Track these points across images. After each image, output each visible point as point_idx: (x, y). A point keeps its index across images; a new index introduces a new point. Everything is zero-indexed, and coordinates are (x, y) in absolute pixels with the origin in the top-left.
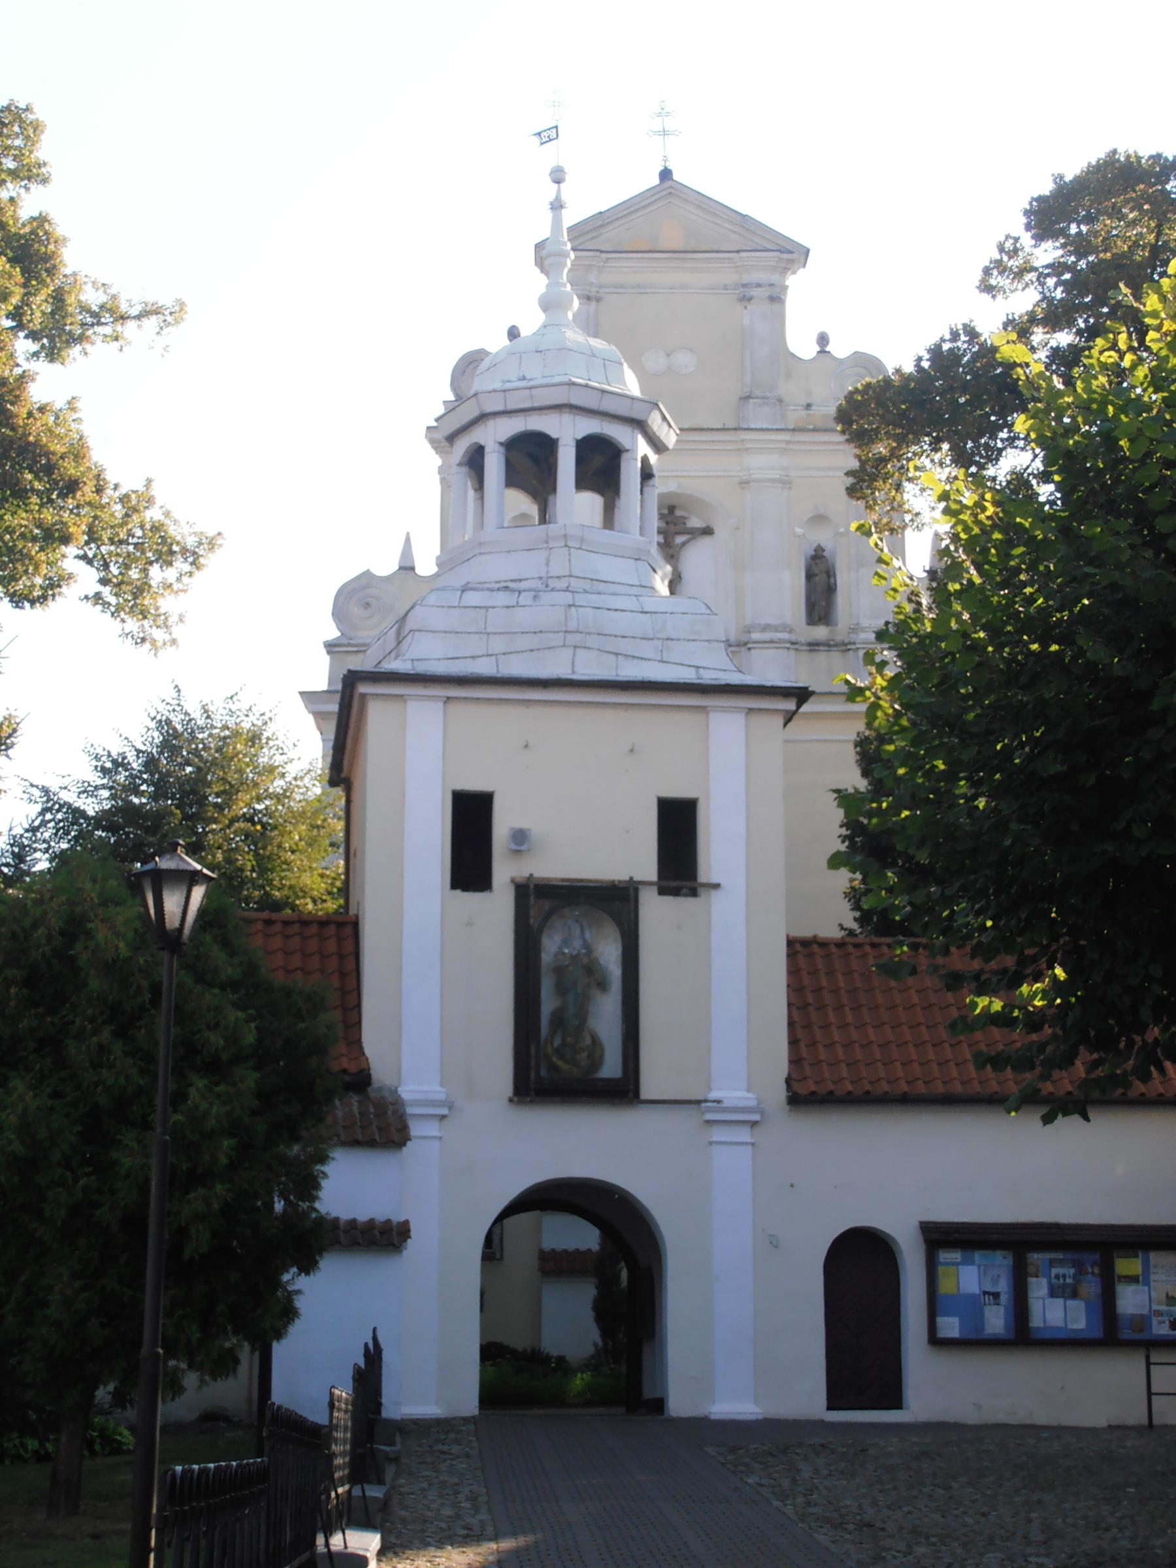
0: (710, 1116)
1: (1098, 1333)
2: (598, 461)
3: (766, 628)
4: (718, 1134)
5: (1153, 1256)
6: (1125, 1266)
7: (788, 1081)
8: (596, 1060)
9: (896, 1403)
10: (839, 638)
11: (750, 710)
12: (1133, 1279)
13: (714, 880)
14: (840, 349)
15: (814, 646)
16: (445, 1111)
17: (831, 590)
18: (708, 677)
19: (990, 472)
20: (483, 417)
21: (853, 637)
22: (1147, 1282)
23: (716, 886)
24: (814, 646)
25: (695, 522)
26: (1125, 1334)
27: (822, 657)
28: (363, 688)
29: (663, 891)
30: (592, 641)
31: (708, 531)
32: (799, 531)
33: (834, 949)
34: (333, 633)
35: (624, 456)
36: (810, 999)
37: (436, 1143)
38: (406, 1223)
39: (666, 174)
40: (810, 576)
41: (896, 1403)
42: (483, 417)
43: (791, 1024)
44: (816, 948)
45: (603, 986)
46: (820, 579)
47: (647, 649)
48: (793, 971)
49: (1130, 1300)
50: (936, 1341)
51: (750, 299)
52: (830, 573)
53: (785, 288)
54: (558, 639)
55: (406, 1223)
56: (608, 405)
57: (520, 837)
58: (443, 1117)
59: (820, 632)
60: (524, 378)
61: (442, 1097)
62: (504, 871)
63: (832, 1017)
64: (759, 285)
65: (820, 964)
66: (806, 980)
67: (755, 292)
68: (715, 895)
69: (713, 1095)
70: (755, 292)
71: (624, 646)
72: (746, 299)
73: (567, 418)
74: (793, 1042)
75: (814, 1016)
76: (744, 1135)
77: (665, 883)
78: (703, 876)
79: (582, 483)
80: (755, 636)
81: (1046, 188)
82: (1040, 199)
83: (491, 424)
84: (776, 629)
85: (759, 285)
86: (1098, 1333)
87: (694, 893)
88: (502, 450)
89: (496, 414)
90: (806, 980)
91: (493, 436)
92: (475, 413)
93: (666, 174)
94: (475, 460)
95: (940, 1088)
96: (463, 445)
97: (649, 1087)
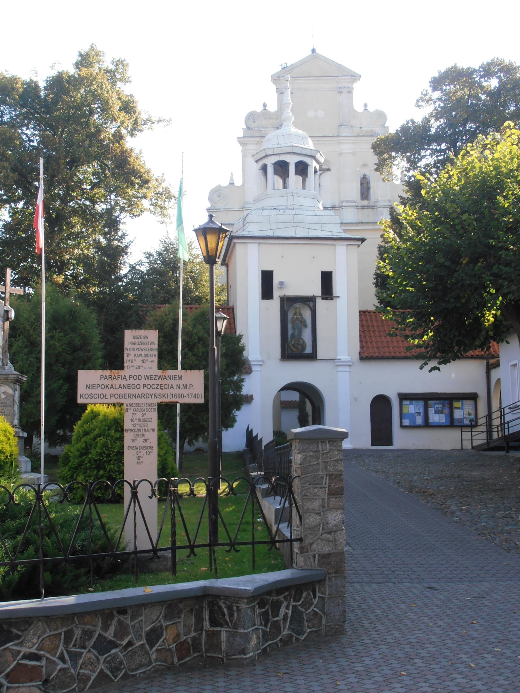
0: (337, 364)
1: (448, 424)
2: (301, 167)
3: (348, 202)
4: (340, 369)
5: (464, 401)
6: (456, 404)
7: (360, 353)
8: (304, 347)
9: (391, 444)
10: (371, 204)
11: (348, 245)
12: (459, 408)
13: (338, 295)
14: (371, 109)
15: (363, 207)
16: (261, 363)
17: (369, 188)
18: (335, 235)
19: (418, 165)
20: (266, 156)
21: (376, 204)
22: (463, 409)
23: (339, 297)
24: (363, 207)
26: (456, 424)
27: (366, 211)
28: (235, 241)
29: (323, 299)
30: (301, 225)
31: (329, 170)
32: (358, 169)
33: (372, 314)
34: (209, 205)
35: (309, 167)
36: (366, 328)
37: (259, 372)
38: (252, 395)
39: (313, 51)
40: (362, 184)
41: (391, 444)
42: (266, 156)
43: (360, 336)
44: (367, 313)
45: (306, 326)
46: (365, 185)
47: (317, 227)
48: (361, 321)
49: (458, 414)
50: (402, 426)
51: (342, 92)
52: (368, 183)
53: (353, 88)
55: (252, 395)
56: (304, 152)
57: (281, 284)
58: (261, 365)
59: (365, 203)
60: (279, 144)
61: (261, 359)
62: (277, 293)
63: (372, 334)
64: (344, 88)
65: (368, 318)
66: (364, 323)
67: (343, 90)
68: (338, 299)
69: (338, 357)
70: (343, 90)
72: (340, 92)
73: (292, 156)
74: (361, 341)
75: (367, 334)
76: (347, 369)
77: (323, 296)
78: (334, 295)
79: (297, 173)
80: (344, 204)
81: (437, 75)
82: (434, 78)
83: (269, 158)
84: (351, 202)
85: (344, 88)
86: (448, 424)
87: (332, 299)
88: (273, 166)
89: (271, 155)
90: (364, 323)
91: (270, 162)
92: (265, 155)
93: (313, 51)
94: (264, 168)
96: (261, 163)
97: (320, 354)
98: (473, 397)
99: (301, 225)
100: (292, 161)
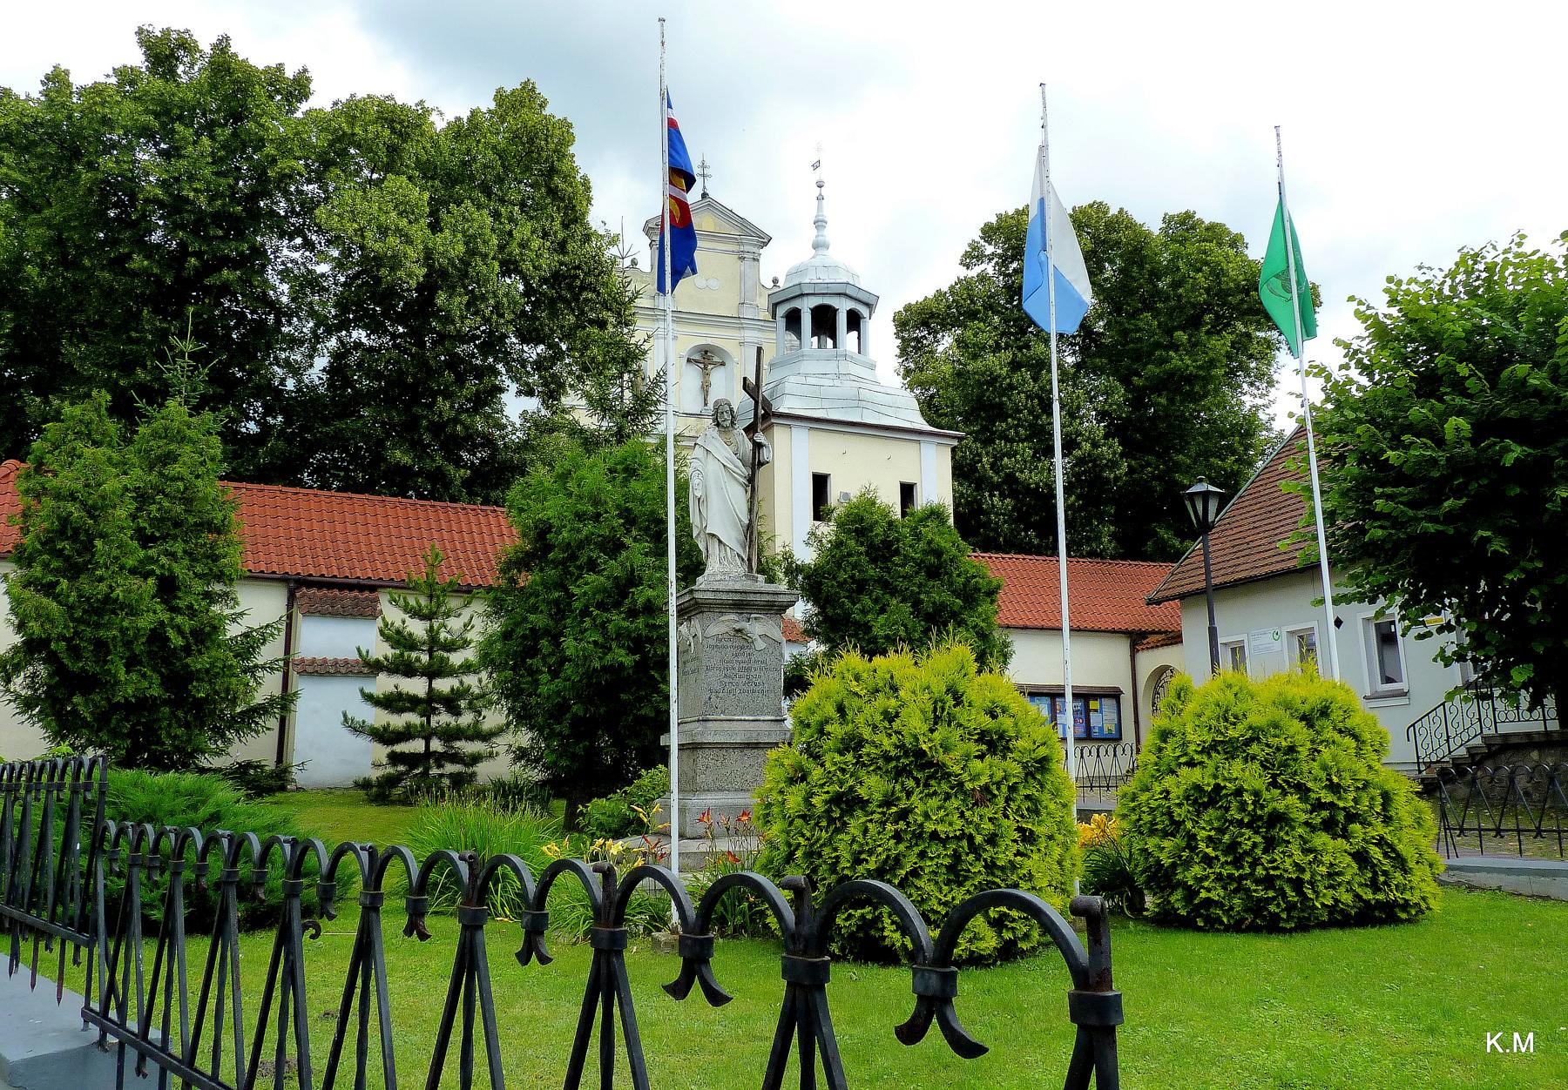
1: (1084, 736)
6: (1093, 705)
12: (1096, 711)
25: (716, 359)
26: (1094, 735)
30: (869, 405)
31: (723, 364)
47: (889, 411)
49: (1095, 719)
54: (855, 403)
56: (860, 296)
71: (882, 409)
73: (843, 299)
83: (805, 298)
86: (1084, 736)
91: (806, 307)
95: (1021, 623)
96: (781, 311)
98: (1115, 694)
99: (869, 405)
100: (843, 307)
